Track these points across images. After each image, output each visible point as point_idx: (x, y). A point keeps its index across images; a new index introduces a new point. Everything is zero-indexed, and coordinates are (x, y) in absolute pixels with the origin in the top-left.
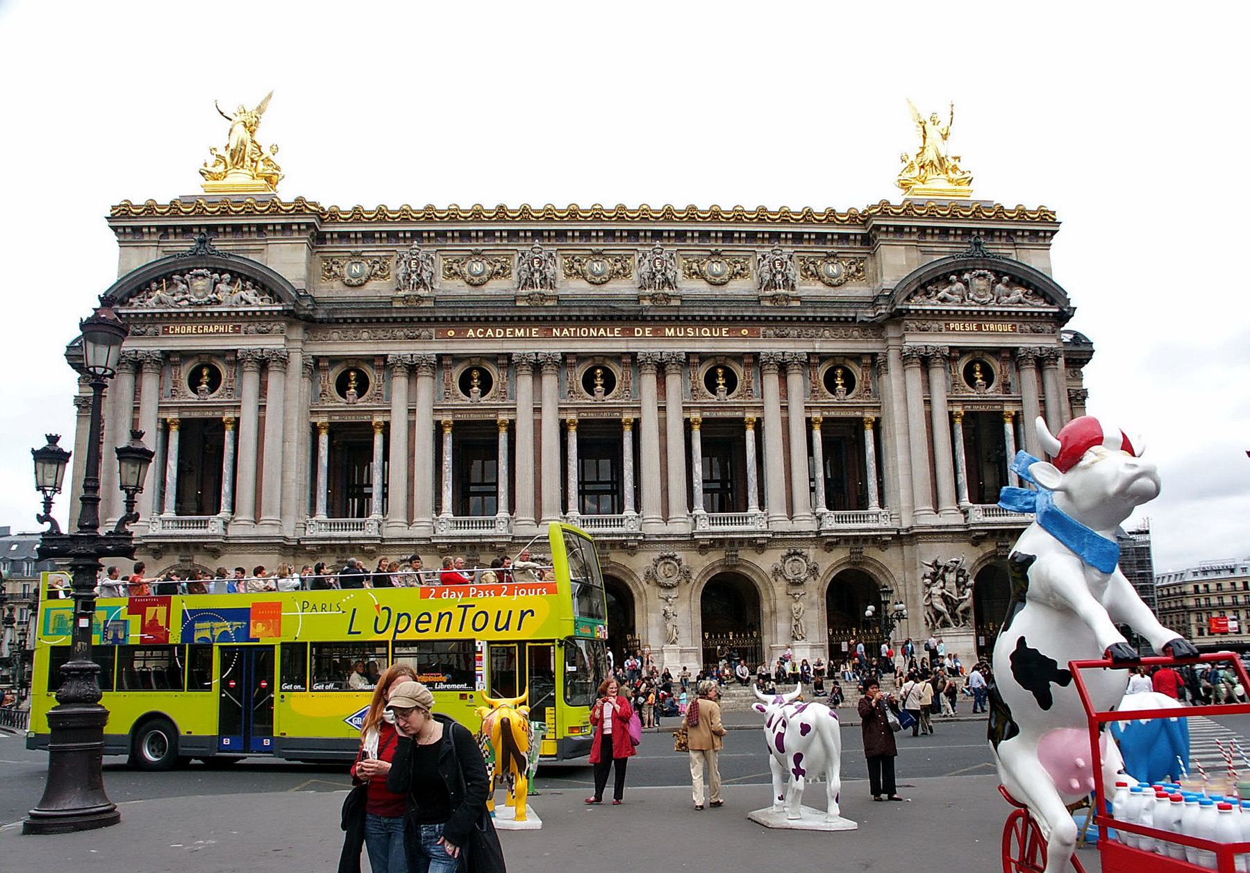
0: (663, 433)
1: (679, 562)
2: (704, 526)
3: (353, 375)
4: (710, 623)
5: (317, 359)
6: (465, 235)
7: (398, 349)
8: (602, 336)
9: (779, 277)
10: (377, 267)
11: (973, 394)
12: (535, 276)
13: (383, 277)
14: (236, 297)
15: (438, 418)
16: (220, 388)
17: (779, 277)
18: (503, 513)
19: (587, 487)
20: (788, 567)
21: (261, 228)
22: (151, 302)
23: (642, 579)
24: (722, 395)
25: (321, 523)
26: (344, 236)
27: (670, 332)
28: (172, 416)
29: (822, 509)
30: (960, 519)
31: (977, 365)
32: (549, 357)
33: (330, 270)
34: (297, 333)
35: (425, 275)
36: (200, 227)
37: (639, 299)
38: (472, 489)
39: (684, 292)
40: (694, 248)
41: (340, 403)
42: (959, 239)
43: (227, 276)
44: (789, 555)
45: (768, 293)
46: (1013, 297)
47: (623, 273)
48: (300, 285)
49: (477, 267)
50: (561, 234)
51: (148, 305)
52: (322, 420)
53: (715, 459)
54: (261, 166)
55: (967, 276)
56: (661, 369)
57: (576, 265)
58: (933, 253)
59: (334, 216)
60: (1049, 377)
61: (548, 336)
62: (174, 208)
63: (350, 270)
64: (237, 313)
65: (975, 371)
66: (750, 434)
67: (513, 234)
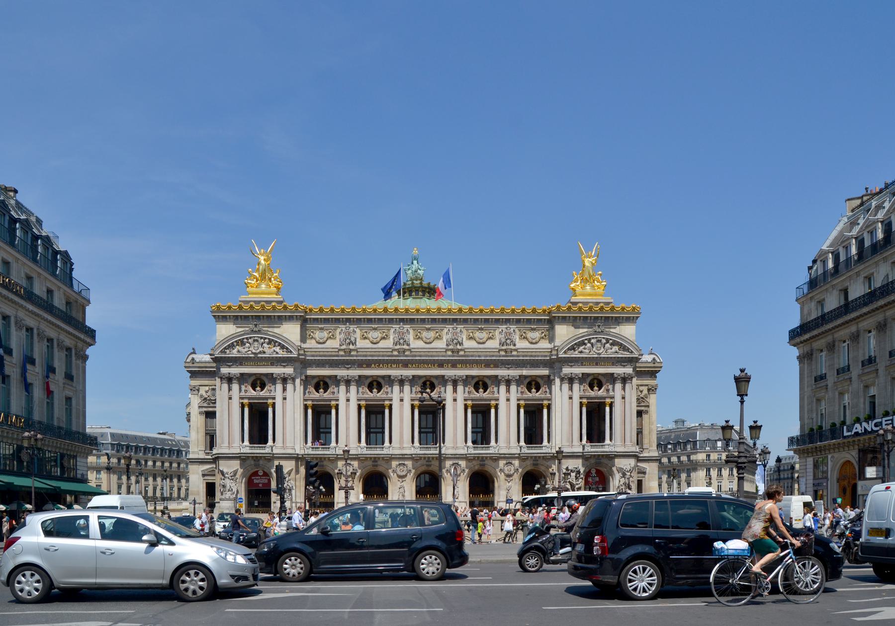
0: (455, 410)
1: (460, 465)
2: (472, 451)
3: (322, 384)
4: (473, 491)
5: (306, 377)
6: (370, 321)
11: (592, 394)
12: (401, 340)
14: (272, 350)
20: (506, 468)
21: (279, 316)
22: (235, 351)
26: (316, 320)
28: (246, 401)
29: (522, 443)
30: (581, 450)
31: (595, 382)
32: (407, 377)
34: (298, 364)
35: (353, 339)
37: (447, 350)
41: (316, 395)
43: (267, 340)
46: (613, 350)
47: (439, 338)
48: (298, 343)
51: (234, 353)
55: (592, 341)
56: (455, 383)
58: (579, 328)
59: (311, 310)
60: (627, 386)
66: (493, 411)
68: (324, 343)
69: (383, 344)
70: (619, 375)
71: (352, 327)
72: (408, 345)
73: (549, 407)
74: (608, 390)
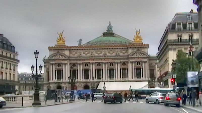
3: (74, 65)
5: (70, 63)
6: (85, 49)
7: (78, 62)
11: (137, 66)
21: (64, 49)
26: (72, 49)
27: (106, 60)
31: (138, 63)
34: (68, 61)
40: (109, 50)
47: (102, 53)
50: (95, 49)
54: (63, 40)
55: (137, 53)
56: (105, 64)
61: (93, 60)
69: (88, 55)
71: (81, 51)
73: (128, 69)
74: (141, 65)
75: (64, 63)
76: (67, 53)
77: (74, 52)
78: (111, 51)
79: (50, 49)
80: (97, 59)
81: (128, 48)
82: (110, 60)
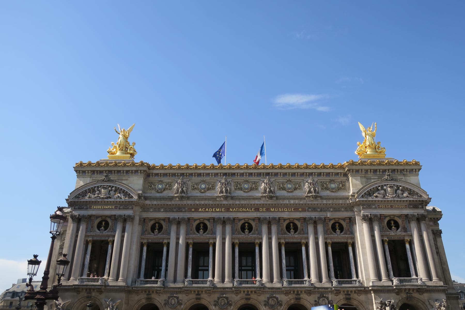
1: (277, 299)
5: (145, 219)
6: (199, 175)
8: (248, 211)
9: (312, 189)
10: (168, 186)
13: (170, 189)
15: (188, 241)
16: (108, 229)
17: (312, 189)
18: (210, 278)
19: (243, 268)
21: (127, 172)
23: (263, 305)
24: (292, 233)
25: (141, 281)
26: (157, 175)
30: (390, 284)
32: (229, 219)
33: (151, 187)
36: (106, 171)
38: (200, 268)
39: (278, 195)
40: (281, 179)
42: (381, 173)
44: (321, 297)
45: (309, 195)
48: (140, 192)
49: (203, 186)
50: (233, 174)
52: (145, 241)
53: (292, 259)
55: (385, 188)
57: (239, 185)
58: (371, 179)
59: (154, 168)
61: (228, 210)
62: (98, 164)
63: (158, 186)
64: (117, 201)
65: (391, 224)
66: (303, 248)
67: (216, 175)
68: (161, 192)
69: (209, 194)
70: (413, 216)
72: (230, 193)
74: (405, 230)
75: (120, 216)
76: (136, 184)
77: (161, 182)
78: (289, 181)
79: (81, 170)
80: (243, 206)
81: (346, 175)
82: (286, 209)
